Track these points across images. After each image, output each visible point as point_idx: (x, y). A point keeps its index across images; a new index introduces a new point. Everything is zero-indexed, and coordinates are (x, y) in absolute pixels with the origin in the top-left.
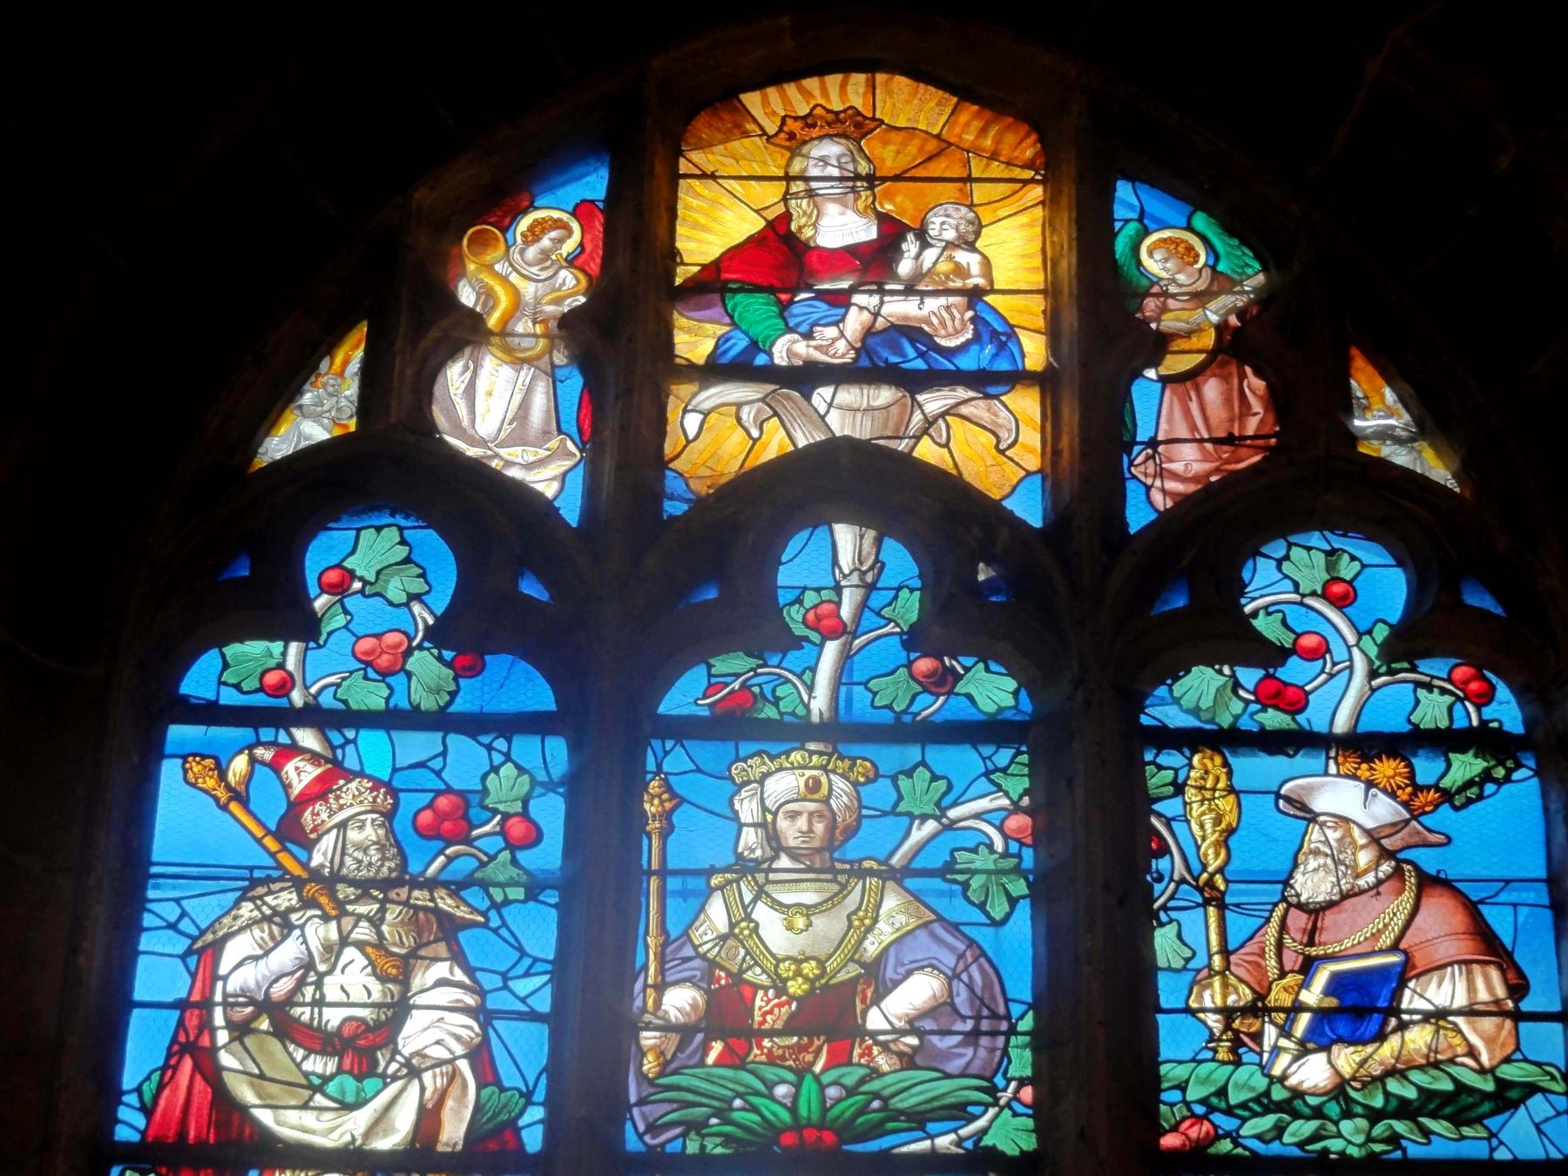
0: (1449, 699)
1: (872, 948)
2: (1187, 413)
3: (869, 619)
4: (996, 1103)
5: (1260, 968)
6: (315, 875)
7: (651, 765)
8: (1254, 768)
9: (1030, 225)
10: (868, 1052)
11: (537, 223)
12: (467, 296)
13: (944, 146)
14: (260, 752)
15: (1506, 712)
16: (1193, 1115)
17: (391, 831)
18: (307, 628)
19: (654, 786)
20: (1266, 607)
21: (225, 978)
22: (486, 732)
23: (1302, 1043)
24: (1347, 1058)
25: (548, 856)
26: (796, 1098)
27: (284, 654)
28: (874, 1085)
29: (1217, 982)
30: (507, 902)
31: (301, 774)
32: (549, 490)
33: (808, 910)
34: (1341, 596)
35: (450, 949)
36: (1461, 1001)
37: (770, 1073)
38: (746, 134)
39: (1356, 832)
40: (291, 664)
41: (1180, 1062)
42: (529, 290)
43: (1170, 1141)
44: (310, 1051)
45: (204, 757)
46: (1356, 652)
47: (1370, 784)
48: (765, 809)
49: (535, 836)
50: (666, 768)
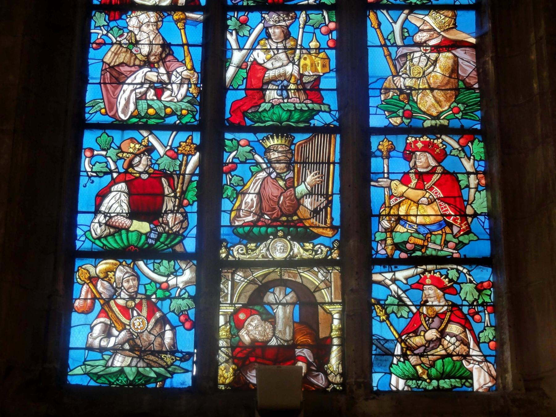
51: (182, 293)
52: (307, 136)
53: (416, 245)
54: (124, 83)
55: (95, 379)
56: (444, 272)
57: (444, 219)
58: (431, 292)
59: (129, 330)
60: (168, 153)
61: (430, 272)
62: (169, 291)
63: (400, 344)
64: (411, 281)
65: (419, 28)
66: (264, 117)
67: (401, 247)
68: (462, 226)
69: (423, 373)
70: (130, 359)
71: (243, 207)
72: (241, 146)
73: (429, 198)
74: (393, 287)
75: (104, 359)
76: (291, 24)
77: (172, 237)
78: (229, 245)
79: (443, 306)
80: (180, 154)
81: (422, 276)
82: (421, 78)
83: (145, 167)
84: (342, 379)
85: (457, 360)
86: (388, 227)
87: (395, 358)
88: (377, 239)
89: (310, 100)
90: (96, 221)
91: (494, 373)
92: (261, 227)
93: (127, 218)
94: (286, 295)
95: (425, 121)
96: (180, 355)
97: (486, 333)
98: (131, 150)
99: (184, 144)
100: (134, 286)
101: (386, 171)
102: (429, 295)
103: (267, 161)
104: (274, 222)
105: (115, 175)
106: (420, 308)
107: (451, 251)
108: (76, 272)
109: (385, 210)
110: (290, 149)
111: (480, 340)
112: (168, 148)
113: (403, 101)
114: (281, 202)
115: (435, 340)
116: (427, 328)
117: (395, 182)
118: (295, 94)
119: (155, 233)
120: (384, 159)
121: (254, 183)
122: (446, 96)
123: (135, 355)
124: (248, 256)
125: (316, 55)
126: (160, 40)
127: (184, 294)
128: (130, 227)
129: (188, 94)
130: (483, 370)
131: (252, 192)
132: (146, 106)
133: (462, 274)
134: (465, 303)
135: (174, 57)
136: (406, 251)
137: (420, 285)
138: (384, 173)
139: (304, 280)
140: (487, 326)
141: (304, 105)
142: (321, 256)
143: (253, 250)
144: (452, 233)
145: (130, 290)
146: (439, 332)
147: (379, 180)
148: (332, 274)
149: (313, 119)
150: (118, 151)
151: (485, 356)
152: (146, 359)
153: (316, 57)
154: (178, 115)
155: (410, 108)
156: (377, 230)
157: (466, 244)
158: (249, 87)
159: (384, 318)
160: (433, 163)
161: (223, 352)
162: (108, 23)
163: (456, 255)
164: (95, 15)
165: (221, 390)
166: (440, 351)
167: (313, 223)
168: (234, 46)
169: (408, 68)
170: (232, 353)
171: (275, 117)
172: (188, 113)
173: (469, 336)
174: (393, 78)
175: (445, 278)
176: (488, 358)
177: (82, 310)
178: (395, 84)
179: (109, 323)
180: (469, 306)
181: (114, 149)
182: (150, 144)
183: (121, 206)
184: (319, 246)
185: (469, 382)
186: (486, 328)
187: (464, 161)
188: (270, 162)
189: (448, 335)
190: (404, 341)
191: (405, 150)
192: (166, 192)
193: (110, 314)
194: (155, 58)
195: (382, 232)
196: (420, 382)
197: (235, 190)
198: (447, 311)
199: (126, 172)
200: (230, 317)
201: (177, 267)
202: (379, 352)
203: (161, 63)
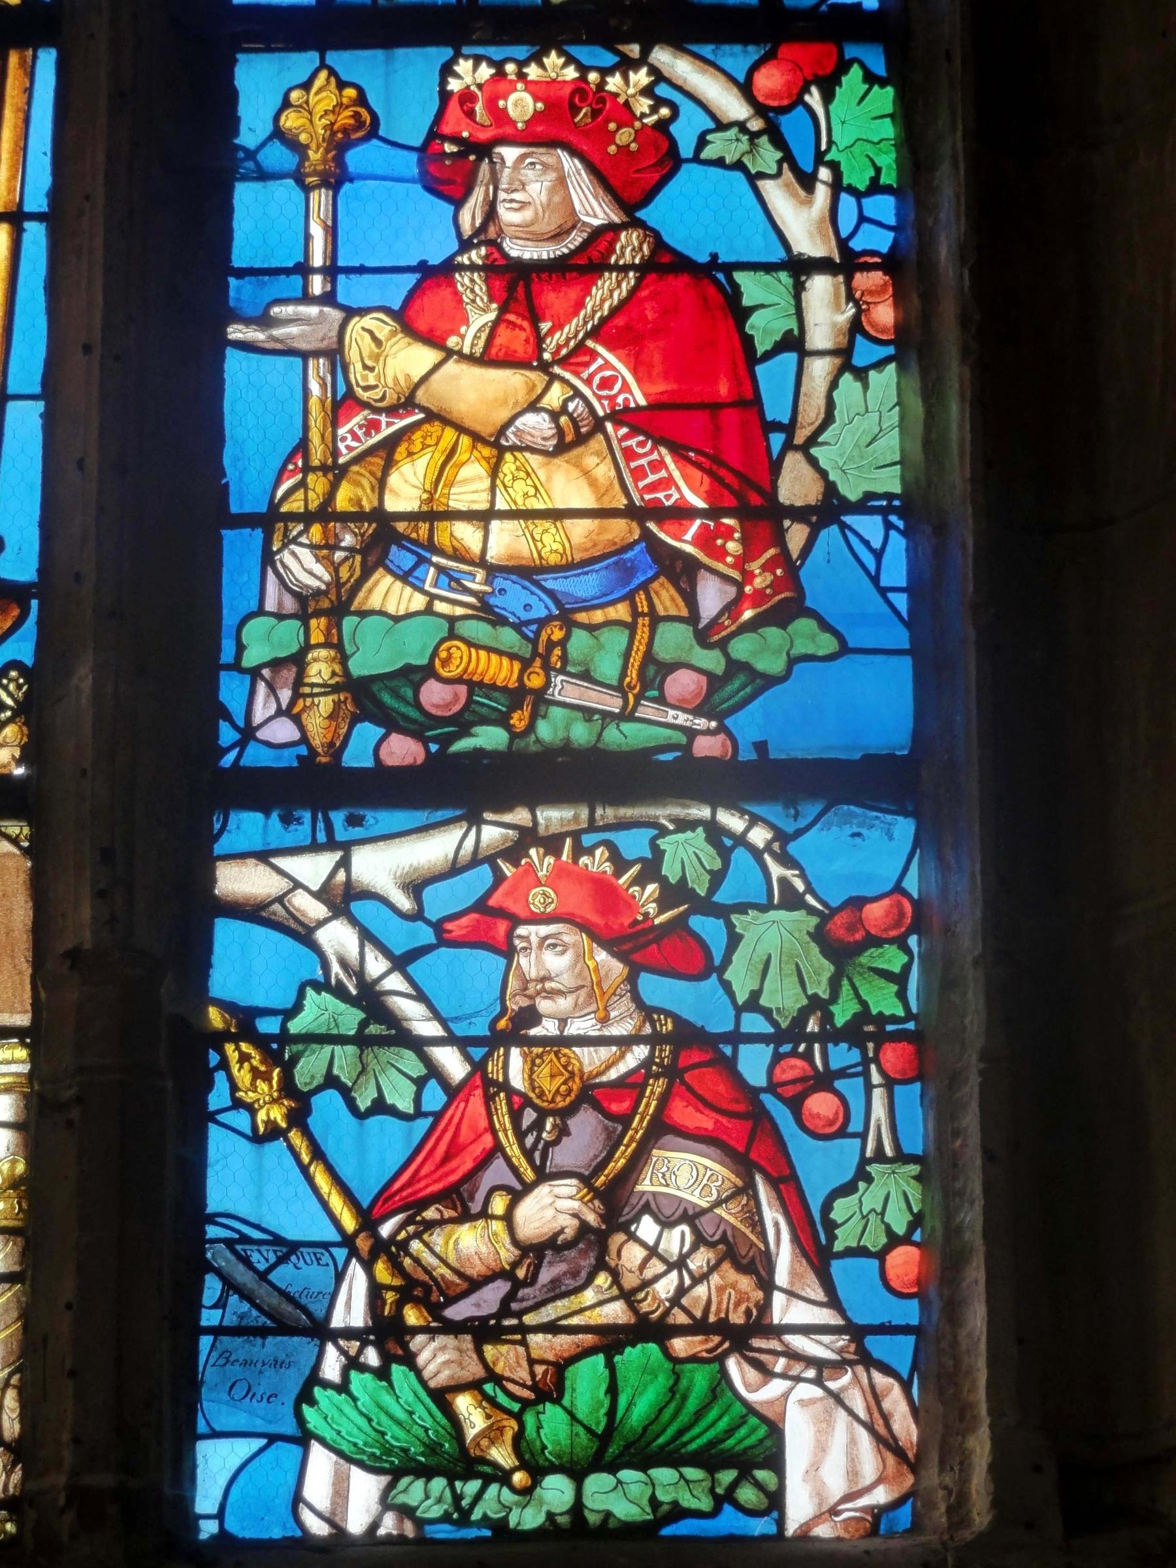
53: (474, 686)
56: (634, 844)
57: (647, 535)
58: (556, 962)
61: (552, 844)
63: (368, 1267)
67: (387, 698)
68: (749, 577)
69: (492, 1434)
73: (564, 410)
79: (625, 1043)
81: (508, 869)
84: (17, 1476)
85: (694, 1359)
86: (315, 583)
87: (331, 1351)
88: (251, 659)
91: (905, 1428)
97: (871, 1197)
101: (318, 260)
102: (543, 980)
106: (489, 1055)
107: (682, 719)
109: (302, 484)
111: (832, 1238)
115: (569, 1245)
116: (529, 1175)
117: (368, 321)
120: (307, 189)
130: (842, 1414)
134: (753, 1023)
138: (303, 269)
140: (880, 1156)
144: (693, 617)
146: (597, 1194)
147: (276, 310)
151: (857, 1332)
157: (771, 681)
159: (277, 1114)
163: (705, 747)
173: (772, 1215)
175: (641, 880)
176: (877, 1345)
180: (777, 1038)
185: (759, 1486)
186: (873, 1169)
187: (776, 194)
189: (647, 1209)
190: (392, 1251)
191: (434, 135)
195: (280, 616)
196: (471, 1487)
198: (649, 1075)
202: (242, 1317)
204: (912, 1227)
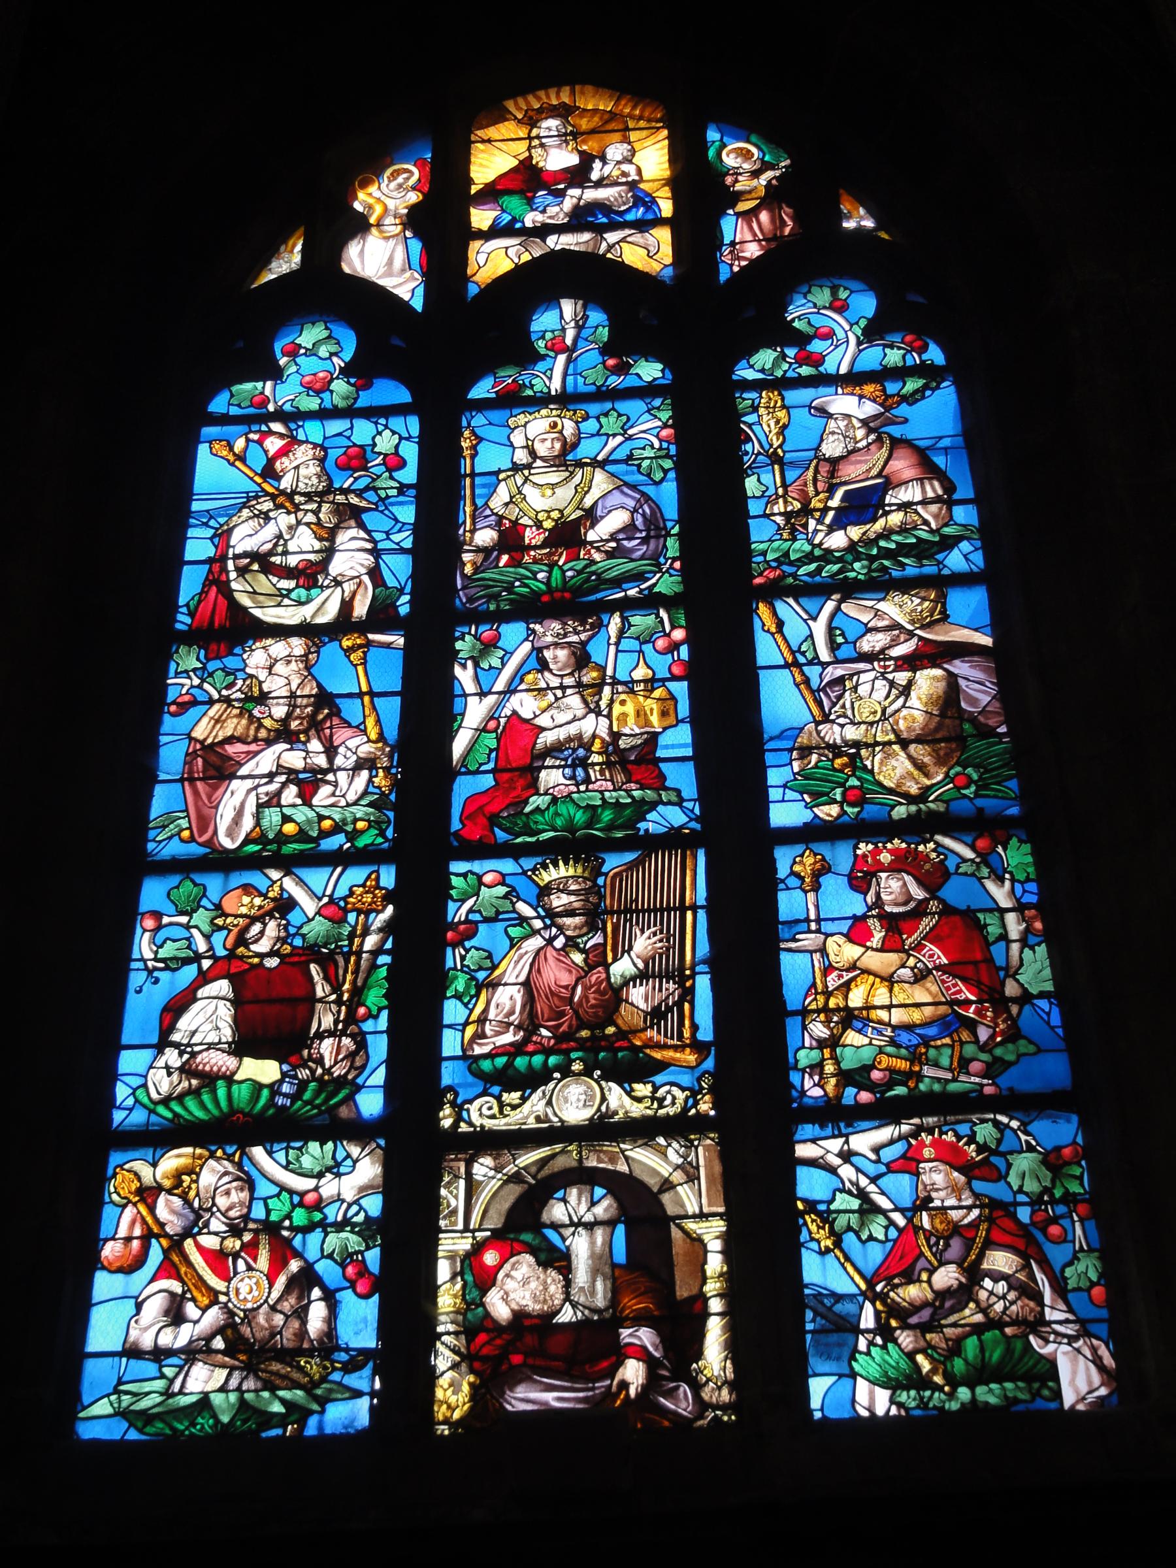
0: (902, 352)
1: (588, 502)
2: (751, 229)
3: (581, 343)
4: (660, 571)
5: (803, 493)
6: (283, 492)
7: (464, 423)
8: (795, 396)
9: (662, 149)
10: (589, 552)
11: (395, 171)
12: (357, 206)
13: (612, 116)
14: (252, 436)
15: (935, 355)
16: (770, 567)
17: (323, 468)
18: (276, 374)
19: (467, 433)
20: (799, 317)
21: (233, 547)
22: (373, 416)
23: (828, 526)
24: (855, 532)
25: (409, 475)
26: (549, 578)
27: (263, 388)
28: (593, 568)
29: (781, 501)
30: (388, 497)
31: (273, 445)
32: (406, 297)
33: (553, 486)
34: (840, 307)
35: (357, 522)
36: (918, 497)
37: (535, 568)
38: (507, 120)
39: (854, 421)
40: (268, 392)
41: (762, 542)
42: (391, 204)
43: (758, 581)
44: (281, 577)
45: (221, 441)
46: (850, 333)
47: (861, 397)
48: (527, 439)
49: (402, 464)
50: (473, 424)
51: (350, 1214)
52: (630, 857)
53: (890, 1070)
54: (233, 776)
55: (140, 1424)
56: (964, 1129)
57: (954, 1011)
59: (226, 1304)
60: (324, 912)
61: (930, 1131)
62: (320, 1210)
64: (888, 1154)
65: (866, 625)
66: (536, 823)
67: (857, 1078)
68: (997, 1025)
69: (934, 1371)
70: (225, 1372)
71: (491, 1016)
72: (486, 886)
73: (915, 967)
74: (847, 1172)
75: (162, 1376)
76: (590, 638)
77: (330, 1089)
78: (459, 1101)
79: (969, 1208)
80: (352, 911)
81: (913, 1142)
82: (878, 722)
83: (272, 942)
84: (734, 1396)
85: (1015, 1336)
87: (861, 1337)
88: (801, 1065)
89: (636, 782)
90: (161, 1063)
91: (1108, 1361)
92: (532, 1054)
93: (229, 1053)
94: (593, 1204)
95: (893, 807)
96: (343, 1357)
97: (1080, 1267)
98: (244, 910)
99: (361, 889)
100: (241, 1204)
101: (812, 916)
102: (933, 1184)
103: (543, 913)
104: (561, 1043)
105: (206, 964)
106: (913, 1216)
107: (977, 1080)
108: (110, 1180)
109: (815, 999)
110: (595, 884)
111: (1067, 1284)
112: (326, 900)
113: (841, 771)
114: (576, 999)
116: (936, 1263)
117: (836, 938)
118: (602, 772)
119: (291, 1083)
121: (517, 962)
122: (938, 754)
123: (237, 1363)
124: (504, 1121)
125: (647, 694)
126: (312, 689)
127: (357, 1214)
128: (234, 1073)
129: (371, 789)
130: (1081, 1357)
131: (512, 980)
132: (279, 818)
133: (1008, 1132)
134: (1021, 1198)
135: (342, 719)
136: (871, 1087)
137: (909, 1164)
138: (807, 920)
139: (634, 1166)
140: (1081, 1249)
141: (622, 793)
142: (671, 1111)
143: (514, 1107)
144: (977, 1041)
145: (232, 1214)
148: (700, 1149)
149: (645, 820)
150: (214, 914)
152: (263, 1371)
153: (646, 697)
154: (347, 833)
155: (857, 783)
156: (800, 1044)
157: (1010, 1064)
158: (502, 764)
159: (829, 1243)
160: (918, 893)
161: (447, 1346)
162: (205, 664)
163: (989, 1090)
164: (177, 652)
165: (442, 1435)
166: (971, 1315)
167: (651, 1038)
168: (470, 687)
169: (848, 705)
170: (468, 1347)
171: (559, 822)
172: (370, 827)
173: (1039, 1276)
174: (817, 726)
175: (968, 1144)
176: (1093, 1328)
177: (118, 1264)
178: (823, 739)
179: (179, 1290)
181: (207, 909)
182: (285, 895)
183: (218, 1028)
184: (667, 1088)
185: (1050, 1389)
186: (1080, 1255)
187: (990, 885)
188: (551, 915)
189: (987, 1275)
190: (883, 1297)
192: (320, 993)
193: (183, 1270)
194: (301, 724)
195: (811, 1048)
196: (928, 1393)
197: (473, 978)
198: (981, 1221)
199: (232, 955)
200: (462, 1262)
201: (340, 1155)
203: (312, 732)
204: (1099, 1278)
